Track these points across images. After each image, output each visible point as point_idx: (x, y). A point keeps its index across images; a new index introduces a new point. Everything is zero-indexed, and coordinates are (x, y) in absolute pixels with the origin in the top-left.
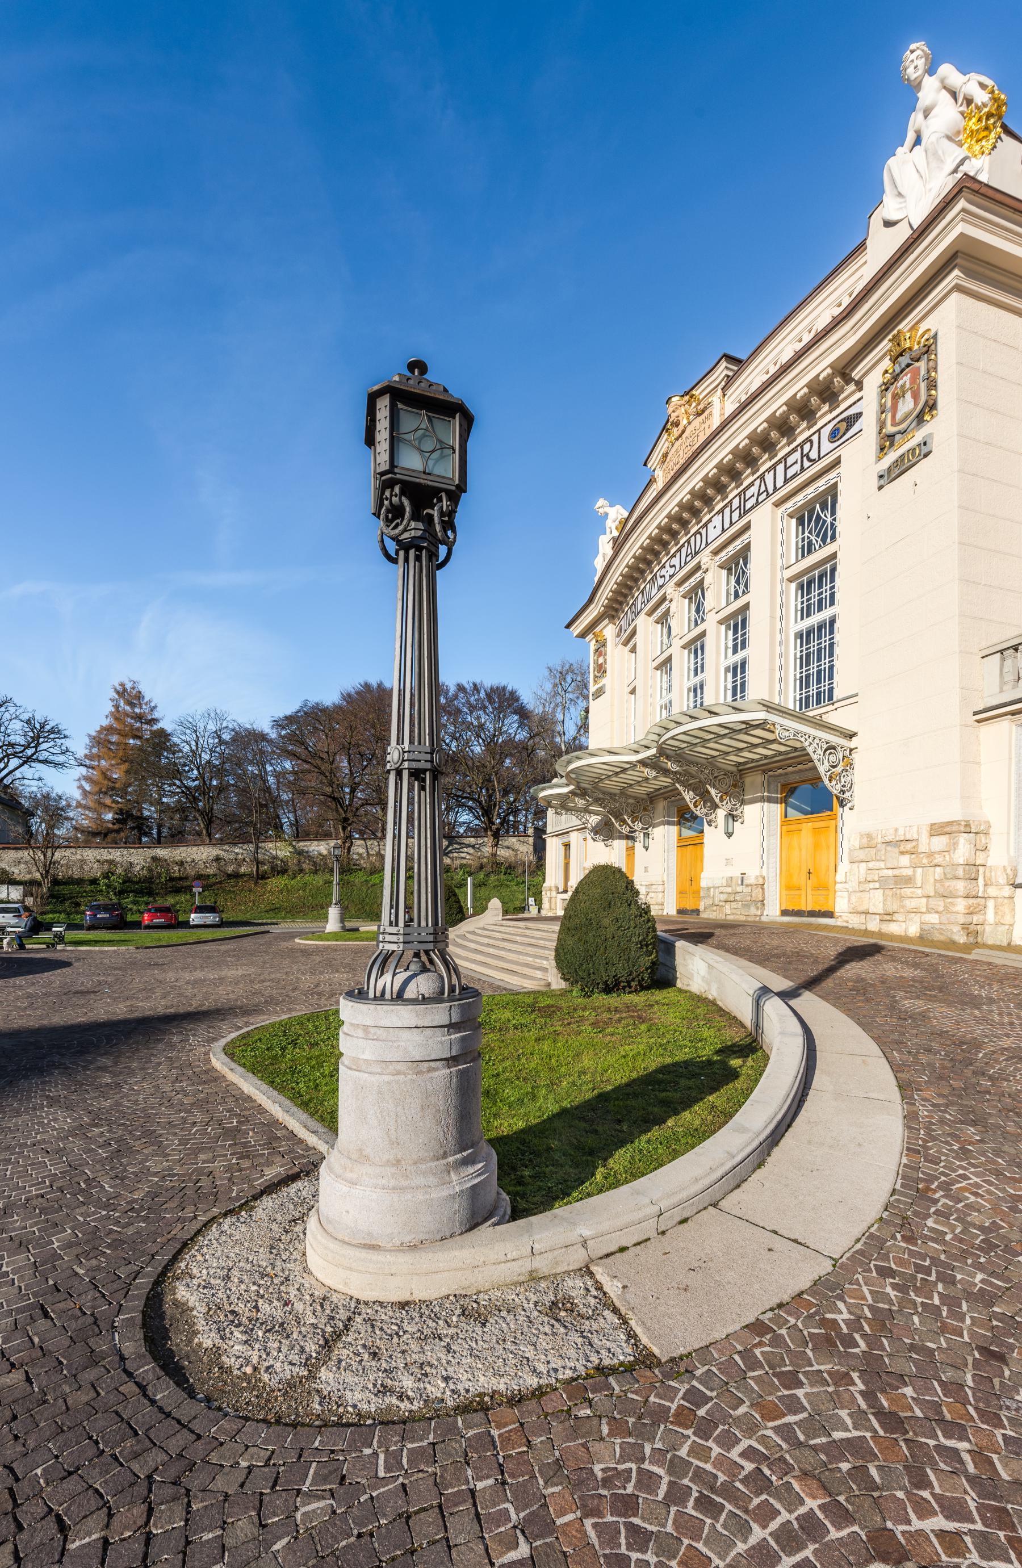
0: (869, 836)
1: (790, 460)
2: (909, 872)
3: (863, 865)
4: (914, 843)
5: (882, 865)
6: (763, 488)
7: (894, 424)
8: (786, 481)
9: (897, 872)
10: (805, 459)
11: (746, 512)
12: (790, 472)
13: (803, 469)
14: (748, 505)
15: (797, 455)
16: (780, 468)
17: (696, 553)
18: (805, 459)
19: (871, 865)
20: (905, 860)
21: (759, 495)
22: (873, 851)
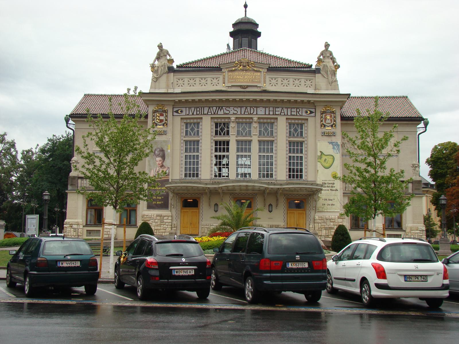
0: (321, 217)
1: (293, 110)
2: (333, 226)
3: (320, 224)
4: (334, 220)
5: (326, 224)
6: (283, 111)
7: (325, 122)
8: (291, 115)
9: (330, 226)
10: (298, 113)
11: (276, 115)
12: (293, 113)
13: (297, 115)
14: (277, 113)
15: (295, 110)
16: (289, 110)
17: (251, 114)
18: (298, 113)
19: (322, 224)
20: (332, 224)
21: (281, 112)
22: (323, 221)
